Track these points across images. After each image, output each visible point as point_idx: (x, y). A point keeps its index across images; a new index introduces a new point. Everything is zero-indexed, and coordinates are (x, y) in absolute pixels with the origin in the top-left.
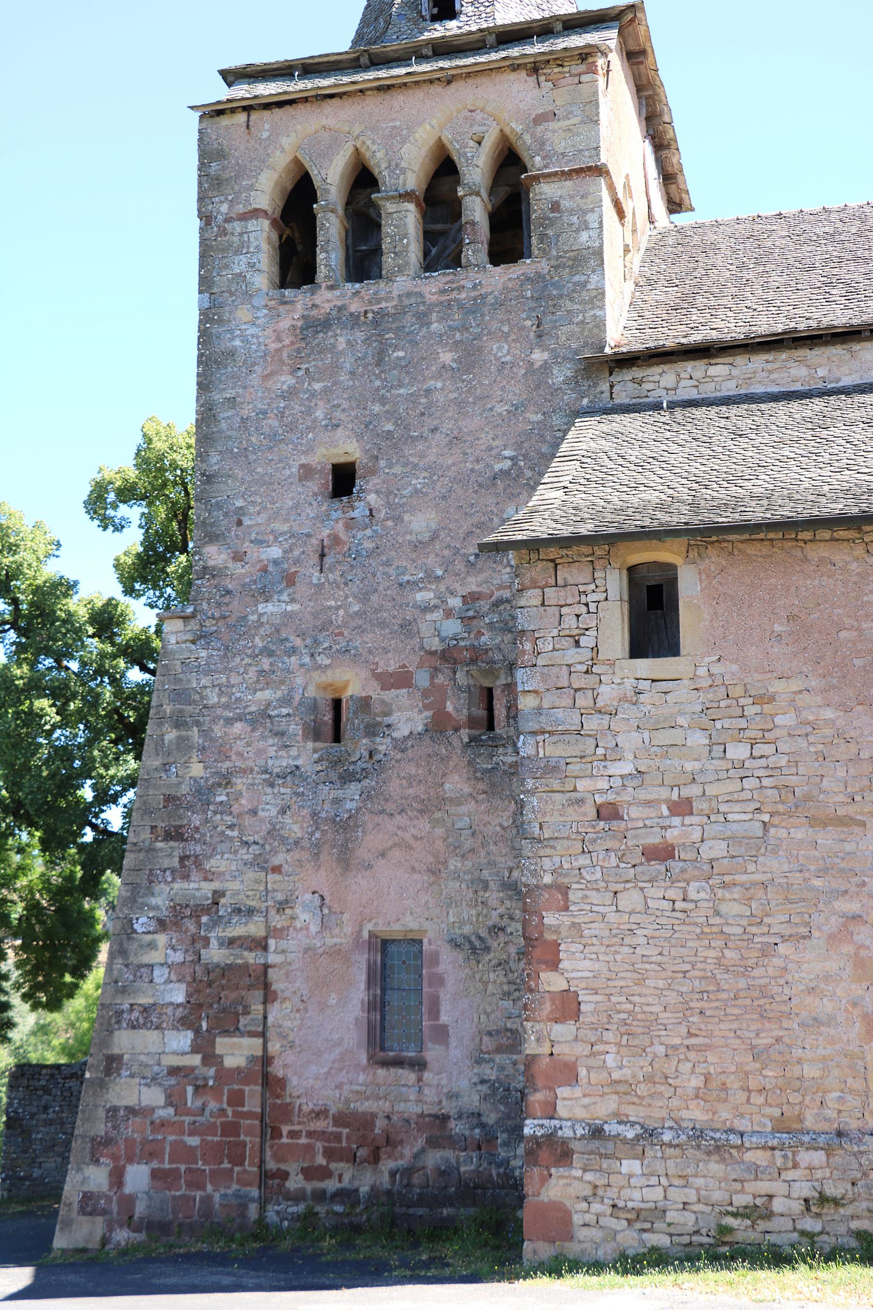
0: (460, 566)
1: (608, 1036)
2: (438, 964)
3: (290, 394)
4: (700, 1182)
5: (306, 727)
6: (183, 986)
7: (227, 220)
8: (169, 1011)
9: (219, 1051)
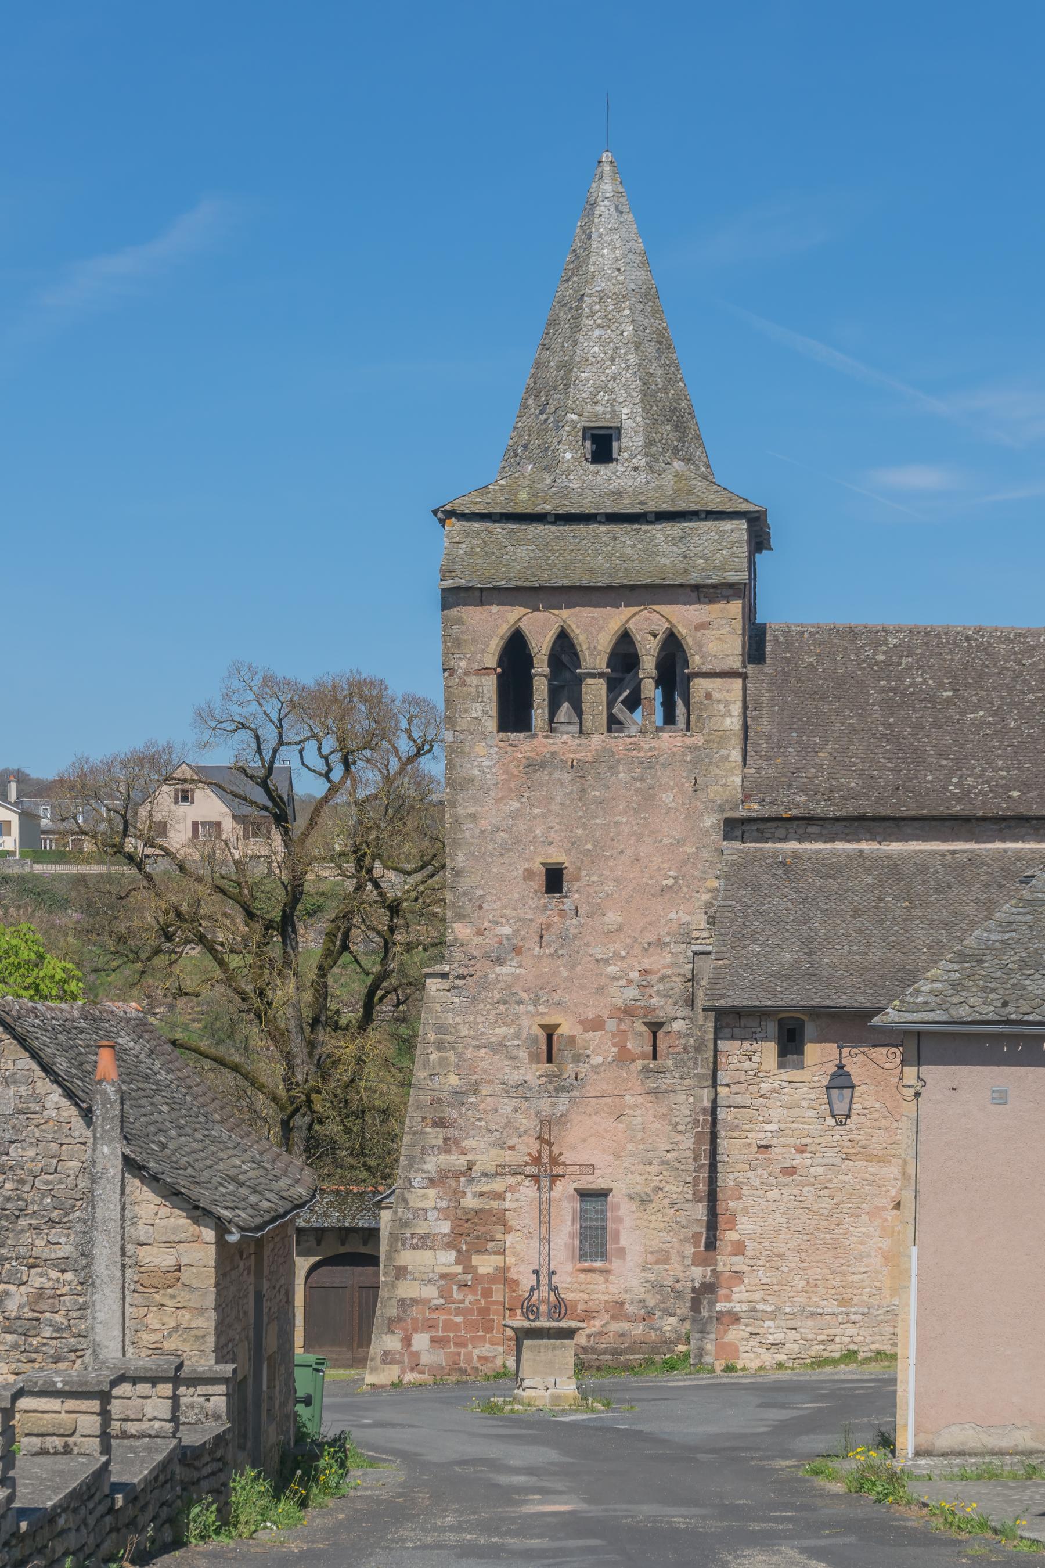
0: (637, 950)
1: (761, 1263)
2: (619, 1209)
3: (516, 814)
4: (802, 1330)
5: (531, 1054)
6: (448, 1223)
7: (466, 674)
8: (439, 1238)
9: (474, 1263)
